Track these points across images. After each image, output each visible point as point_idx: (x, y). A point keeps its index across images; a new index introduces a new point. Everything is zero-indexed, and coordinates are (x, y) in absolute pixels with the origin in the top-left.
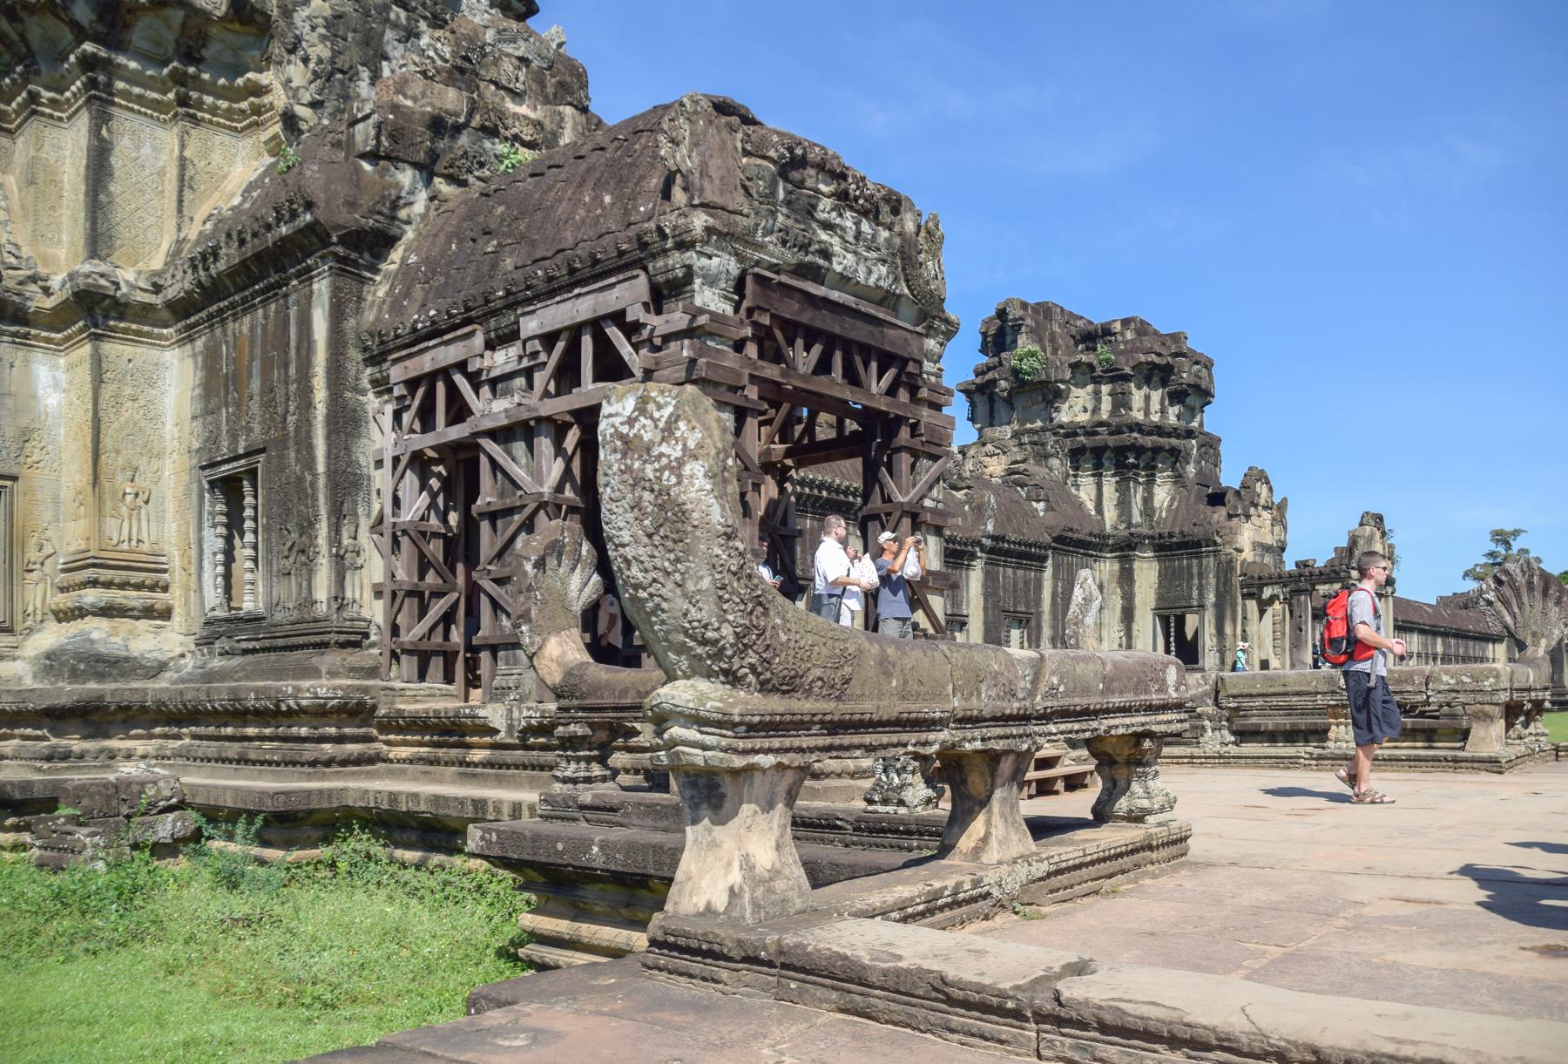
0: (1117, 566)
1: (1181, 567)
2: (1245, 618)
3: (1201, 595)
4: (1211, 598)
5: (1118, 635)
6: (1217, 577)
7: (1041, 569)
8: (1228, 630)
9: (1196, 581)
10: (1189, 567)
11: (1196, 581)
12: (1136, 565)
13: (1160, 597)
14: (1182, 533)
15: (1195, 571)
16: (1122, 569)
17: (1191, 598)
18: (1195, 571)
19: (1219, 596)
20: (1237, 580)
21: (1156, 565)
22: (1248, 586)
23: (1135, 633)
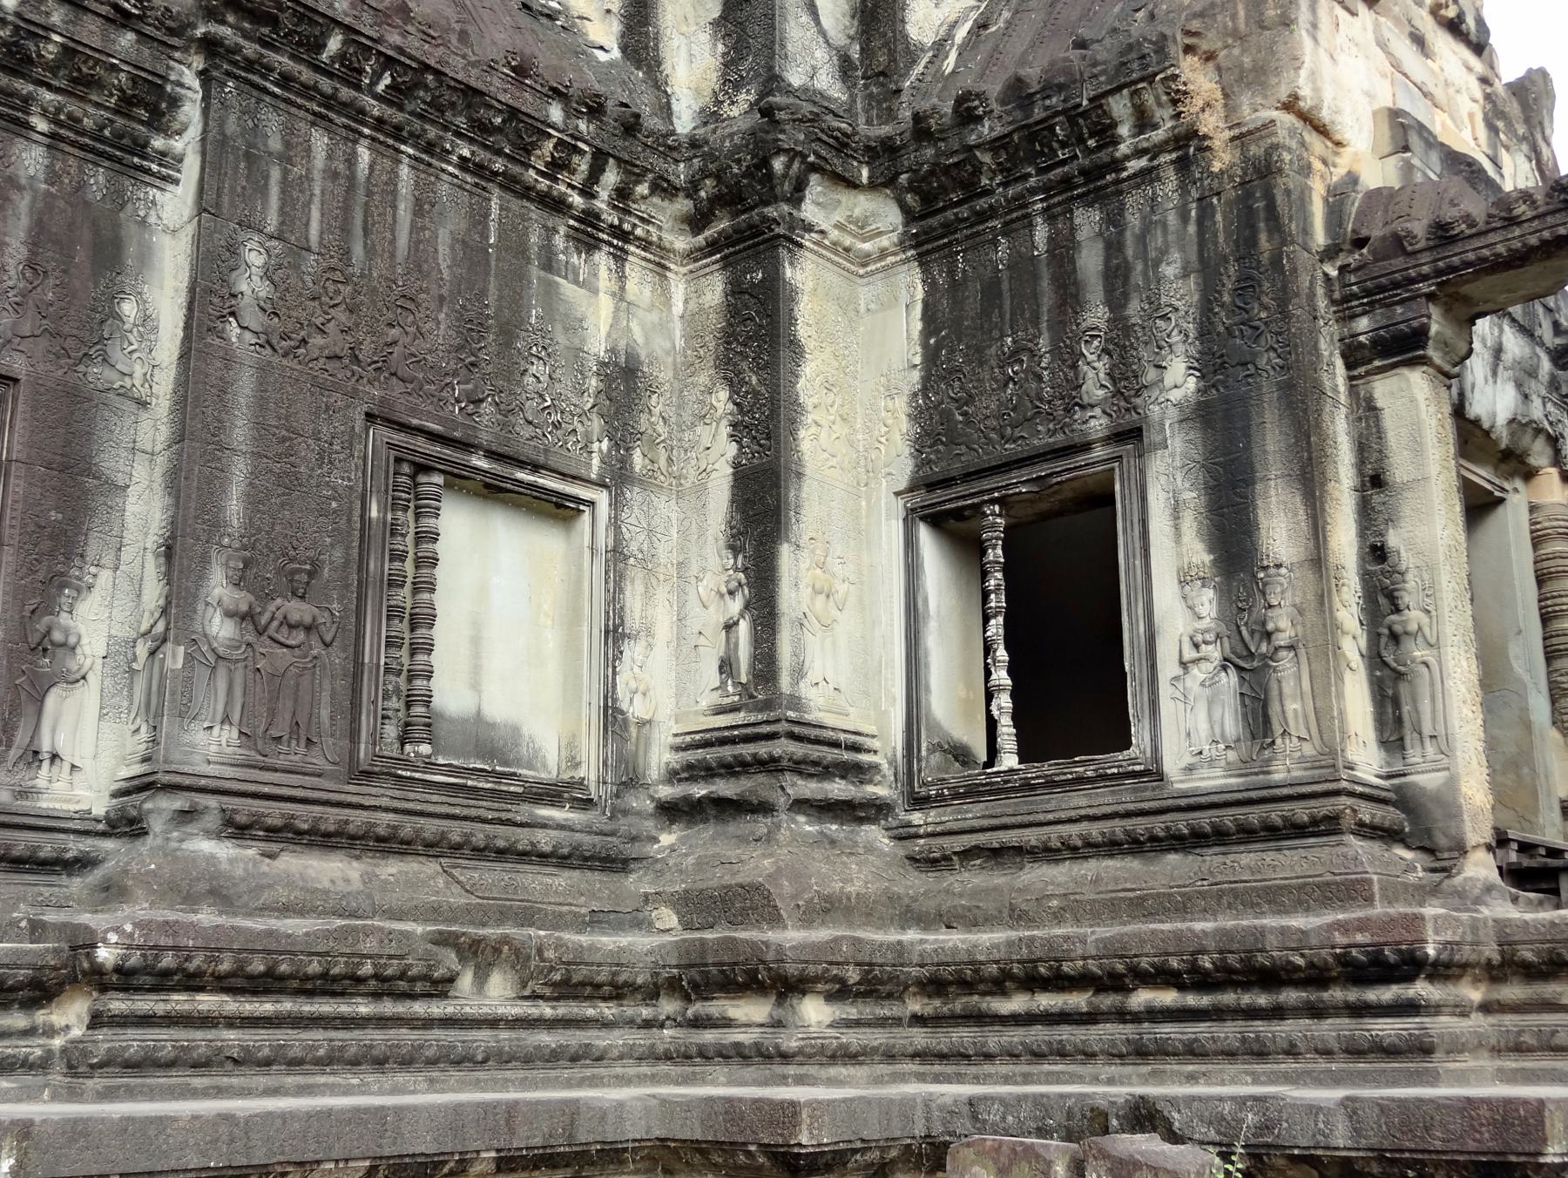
0: (714, 290)
1: (1023, 265)
2: (1374, 481)
3: (1127, 383)
4: (1178, 380)
5: (715, 616)
6: (1207, 269)
7: (130, 155)
8: (1279, 533)
9: (1096, 315)
10: (1063, 250)
11: (1096, 315)
12: (808, 277)
13: (936, 426)
14: (1018, 83)
15: (1090, 261)
16: (736, 290)
17: (1072, 400)
18: (1090, 261)
19: (1213, 364)
20: (1315, 279)
21: (910, 285)
22: (1377, 294)
23: (792, 596)
